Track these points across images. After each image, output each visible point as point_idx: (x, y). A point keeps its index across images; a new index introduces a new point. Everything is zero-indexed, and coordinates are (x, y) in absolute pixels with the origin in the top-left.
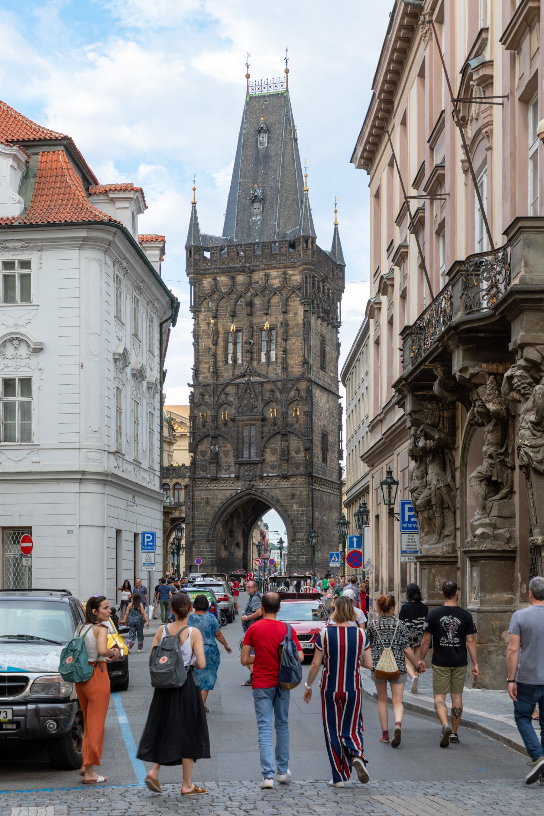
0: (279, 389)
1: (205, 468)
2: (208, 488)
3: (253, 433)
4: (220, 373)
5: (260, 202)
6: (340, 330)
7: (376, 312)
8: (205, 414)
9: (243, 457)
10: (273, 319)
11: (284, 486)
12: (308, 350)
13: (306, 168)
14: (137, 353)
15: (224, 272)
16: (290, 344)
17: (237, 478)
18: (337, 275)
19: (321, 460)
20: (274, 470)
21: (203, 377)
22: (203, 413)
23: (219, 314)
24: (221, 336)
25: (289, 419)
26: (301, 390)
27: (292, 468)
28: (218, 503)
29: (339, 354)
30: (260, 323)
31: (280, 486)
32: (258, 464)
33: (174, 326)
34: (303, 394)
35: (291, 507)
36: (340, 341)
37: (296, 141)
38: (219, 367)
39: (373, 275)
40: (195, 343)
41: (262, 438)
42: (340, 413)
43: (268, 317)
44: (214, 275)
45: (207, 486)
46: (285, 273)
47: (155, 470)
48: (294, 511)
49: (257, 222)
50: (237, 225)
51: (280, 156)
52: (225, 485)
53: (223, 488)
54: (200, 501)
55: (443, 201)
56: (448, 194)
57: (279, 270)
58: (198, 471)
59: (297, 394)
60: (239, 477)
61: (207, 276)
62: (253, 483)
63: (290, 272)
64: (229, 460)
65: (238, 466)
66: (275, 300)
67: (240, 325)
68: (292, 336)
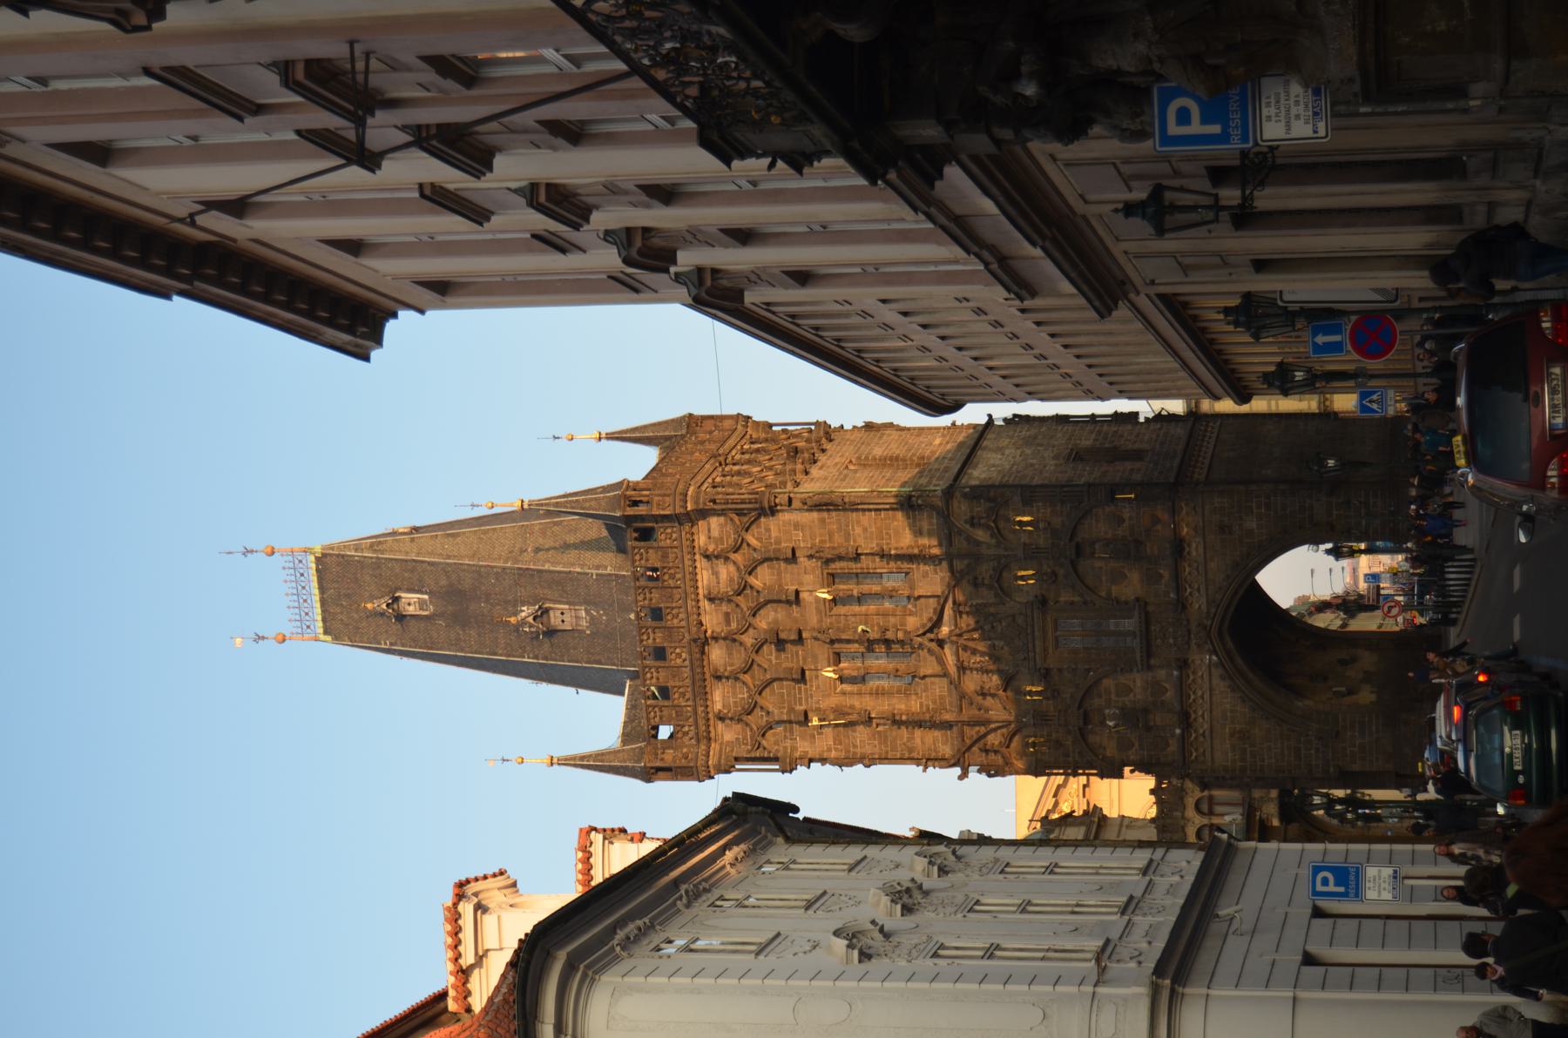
2: (1207, 733)
4: (934, 702)
5: (547, 611)
6: (834, 424)
7: (725, 283)
10: (809, 578)
11: (1201, 550)
12: (879, 497)
13: (473, 505)
14: (852, 902)
15: (701, 693)
16: (866, 538)
17: (1183, 664)
18: (711, 432)
19: (1138, 465)
20: (1161, 576)
21: (945, 743)
23: (798, 708)
24: (849, 701)
25: (1041, 542)
29: (890, 425)
30: (819, 611)
32: (1147, 613)
33: (796, 809)
34: (980, 508)
36: (860, 424)
37: (416, 529)
38: (921, 704)
39: (635, 295)
40: (867, 761)
42: (1027, 419)
44: (711, 716)
47: (1151, 861)
49: (592, 618)
50: (599, 662)
51: (448, 564)
52: (1200, 693)
53: (1207, 696)
55: (374, 64)
56: (352, 44)
57: (698, 564)
59: (983, 521)
60: (1178, 660)
61: (712, 735)
63: (701, 540)
64: (1139, 683)
65: (1152, 662)
68: (847, 536)
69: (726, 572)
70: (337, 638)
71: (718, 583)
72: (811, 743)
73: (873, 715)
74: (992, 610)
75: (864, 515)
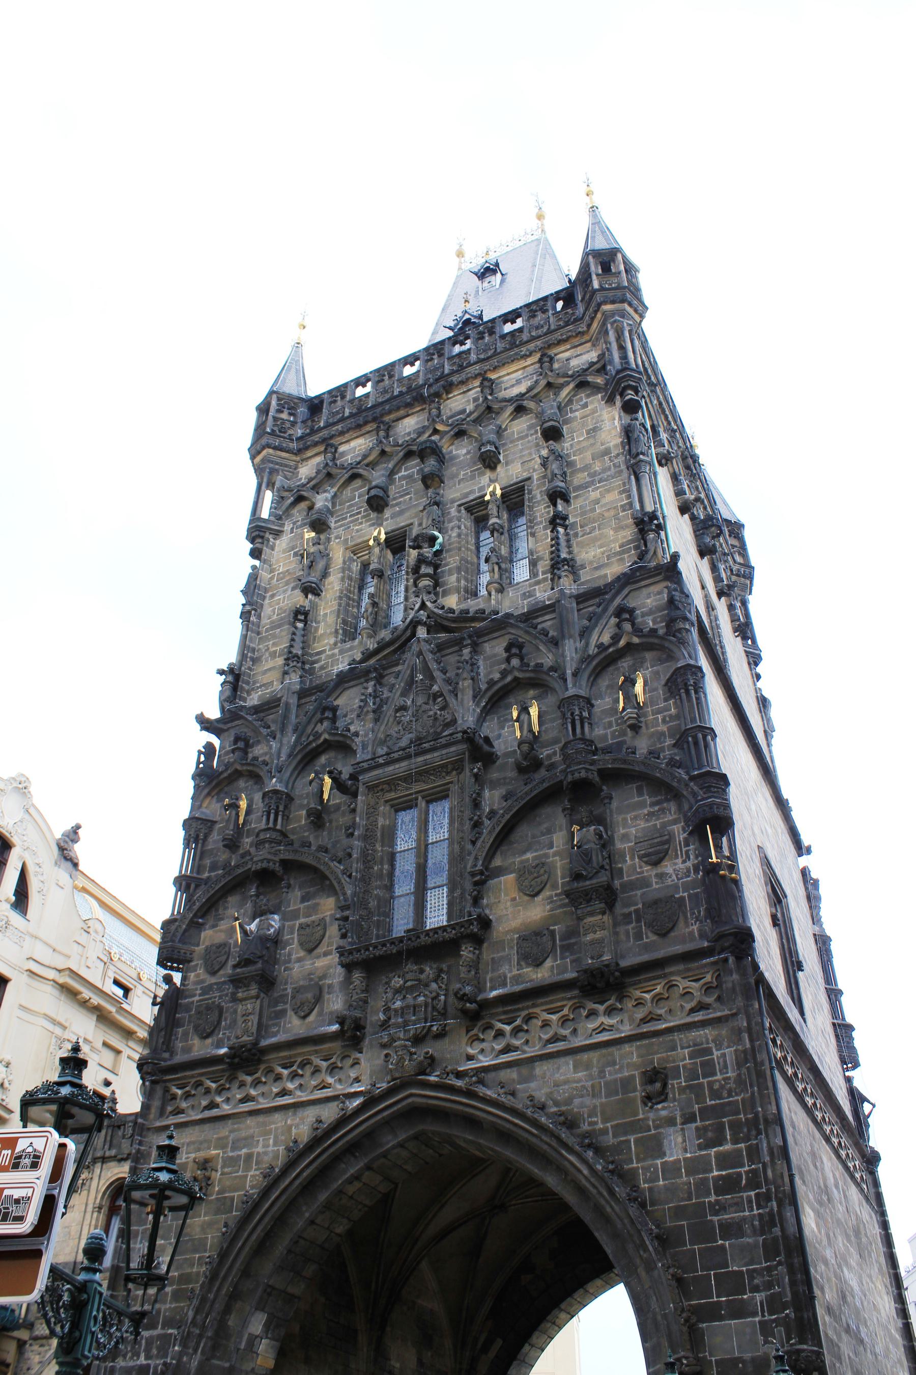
0: (545, 633)
1: (213, 1017)
2: (215, 1112)
4: (322, 668)
8: (243, 804)
20: (538, 964)
22: (237, 799)
26: (644, 615)
27: (639, 936)
31: (578, 1042)
35: (654, 1147)
36: (766, 694)
38: (324, 651)
40: (248, 608)
41: (477, 825)
43: (499, 468)
45: (212, 1105)
46: (546, 360)
48: (671, 1170)
52: (290, 1086)
57: (530, 361)
58: (186, 1034)
59: (627, 627)
61: (309, 453)
62: (430, 1048)
63: (567, 355)
65: (357, 975)
66: (521, 425)
67: (402, 522)
70: (458, 277)
71: (505, 389)
72: (284, 551)
73: (310, 596)
74: (466, 684)
75: (621, 493)
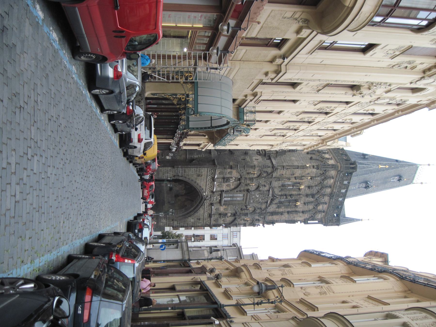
3: (238, 199)
9: (225, 194)
20: (215, 210)
28: (198, 182)
35: (193, 219)
45: (209, 175)
48: (190, 220)
54: (201, 171)
57: (326, 209)
64: (224, 187)
69: (320, 207)
